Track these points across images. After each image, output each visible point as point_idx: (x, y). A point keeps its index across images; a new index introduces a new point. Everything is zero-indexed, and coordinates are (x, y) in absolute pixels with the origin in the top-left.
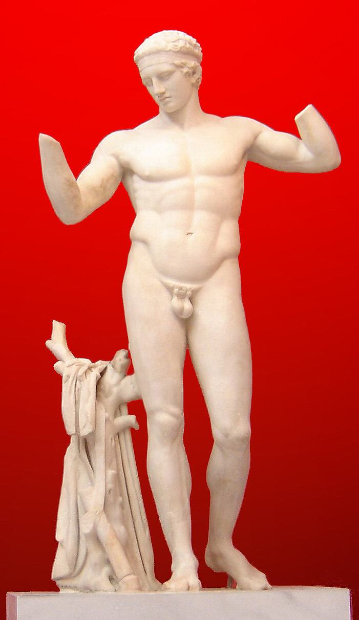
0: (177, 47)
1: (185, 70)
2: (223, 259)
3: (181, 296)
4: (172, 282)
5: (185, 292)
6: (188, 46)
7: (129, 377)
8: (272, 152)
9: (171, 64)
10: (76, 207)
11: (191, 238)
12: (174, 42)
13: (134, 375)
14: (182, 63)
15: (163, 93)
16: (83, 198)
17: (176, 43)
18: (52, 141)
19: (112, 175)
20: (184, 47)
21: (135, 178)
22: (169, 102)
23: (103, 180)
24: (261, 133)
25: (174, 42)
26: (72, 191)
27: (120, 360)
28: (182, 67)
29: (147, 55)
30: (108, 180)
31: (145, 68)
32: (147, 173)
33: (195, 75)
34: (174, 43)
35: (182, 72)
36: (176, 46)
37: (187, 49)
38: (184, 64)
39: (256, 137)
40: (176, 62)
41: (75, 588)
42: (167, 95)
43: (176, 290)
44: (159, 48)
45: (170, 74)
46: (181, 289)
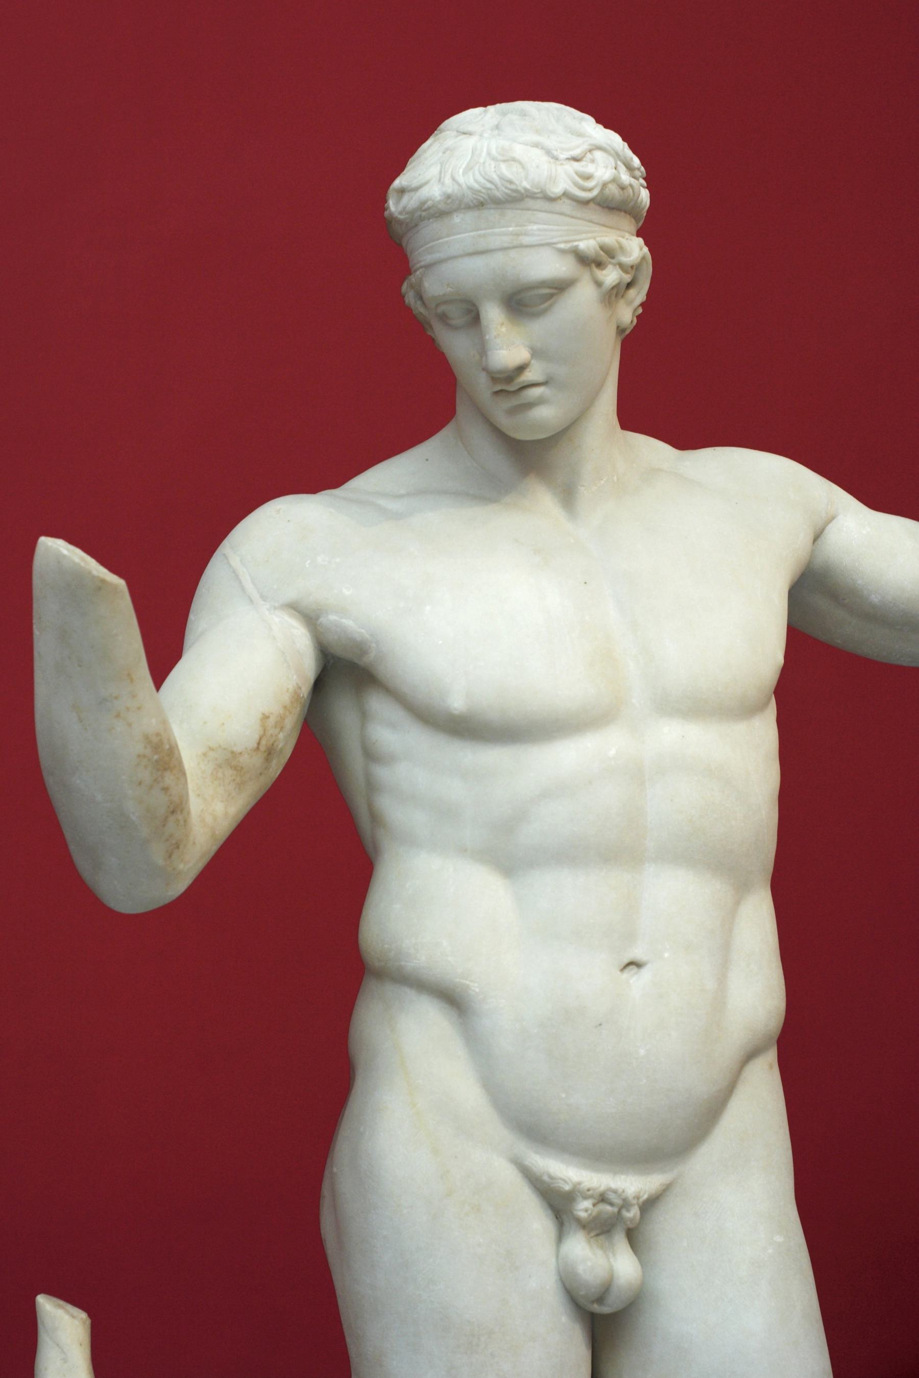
0: (590, 184)
1: (611, 276)
2: (750, 1056)
5: (616, 1210)
6: (625, 178)
8: (875, 599)
9: (562, 252)
10: (175, 847)
11: (638, 981)
12: (576, 159)
14: (603, 248)
15: (521, 369)
16: (195, 805)
17: (586, 167)
18: (103, 581)
19: (296, 695)
20: (614, 180)
21: (378, 704)
22: (540, 401)
23: (265, 717)
24: (831, 519)
25: (576, 159)
26: (166, 789)
28: (600, 265)
29: (469, 207)
30: (280, 725)
32: (457, 703)
33: (632, 292)
34: (575, 164)
35: (598, 284)
36: (588, 177)
37: (623, 188)
38: (609, 252)
39: (817, 537)
40: (583, 245)
42: (529, 376)
43: (583, 1208)
44: (526, 184)
45: (560, 287)
46: (602, 1198)
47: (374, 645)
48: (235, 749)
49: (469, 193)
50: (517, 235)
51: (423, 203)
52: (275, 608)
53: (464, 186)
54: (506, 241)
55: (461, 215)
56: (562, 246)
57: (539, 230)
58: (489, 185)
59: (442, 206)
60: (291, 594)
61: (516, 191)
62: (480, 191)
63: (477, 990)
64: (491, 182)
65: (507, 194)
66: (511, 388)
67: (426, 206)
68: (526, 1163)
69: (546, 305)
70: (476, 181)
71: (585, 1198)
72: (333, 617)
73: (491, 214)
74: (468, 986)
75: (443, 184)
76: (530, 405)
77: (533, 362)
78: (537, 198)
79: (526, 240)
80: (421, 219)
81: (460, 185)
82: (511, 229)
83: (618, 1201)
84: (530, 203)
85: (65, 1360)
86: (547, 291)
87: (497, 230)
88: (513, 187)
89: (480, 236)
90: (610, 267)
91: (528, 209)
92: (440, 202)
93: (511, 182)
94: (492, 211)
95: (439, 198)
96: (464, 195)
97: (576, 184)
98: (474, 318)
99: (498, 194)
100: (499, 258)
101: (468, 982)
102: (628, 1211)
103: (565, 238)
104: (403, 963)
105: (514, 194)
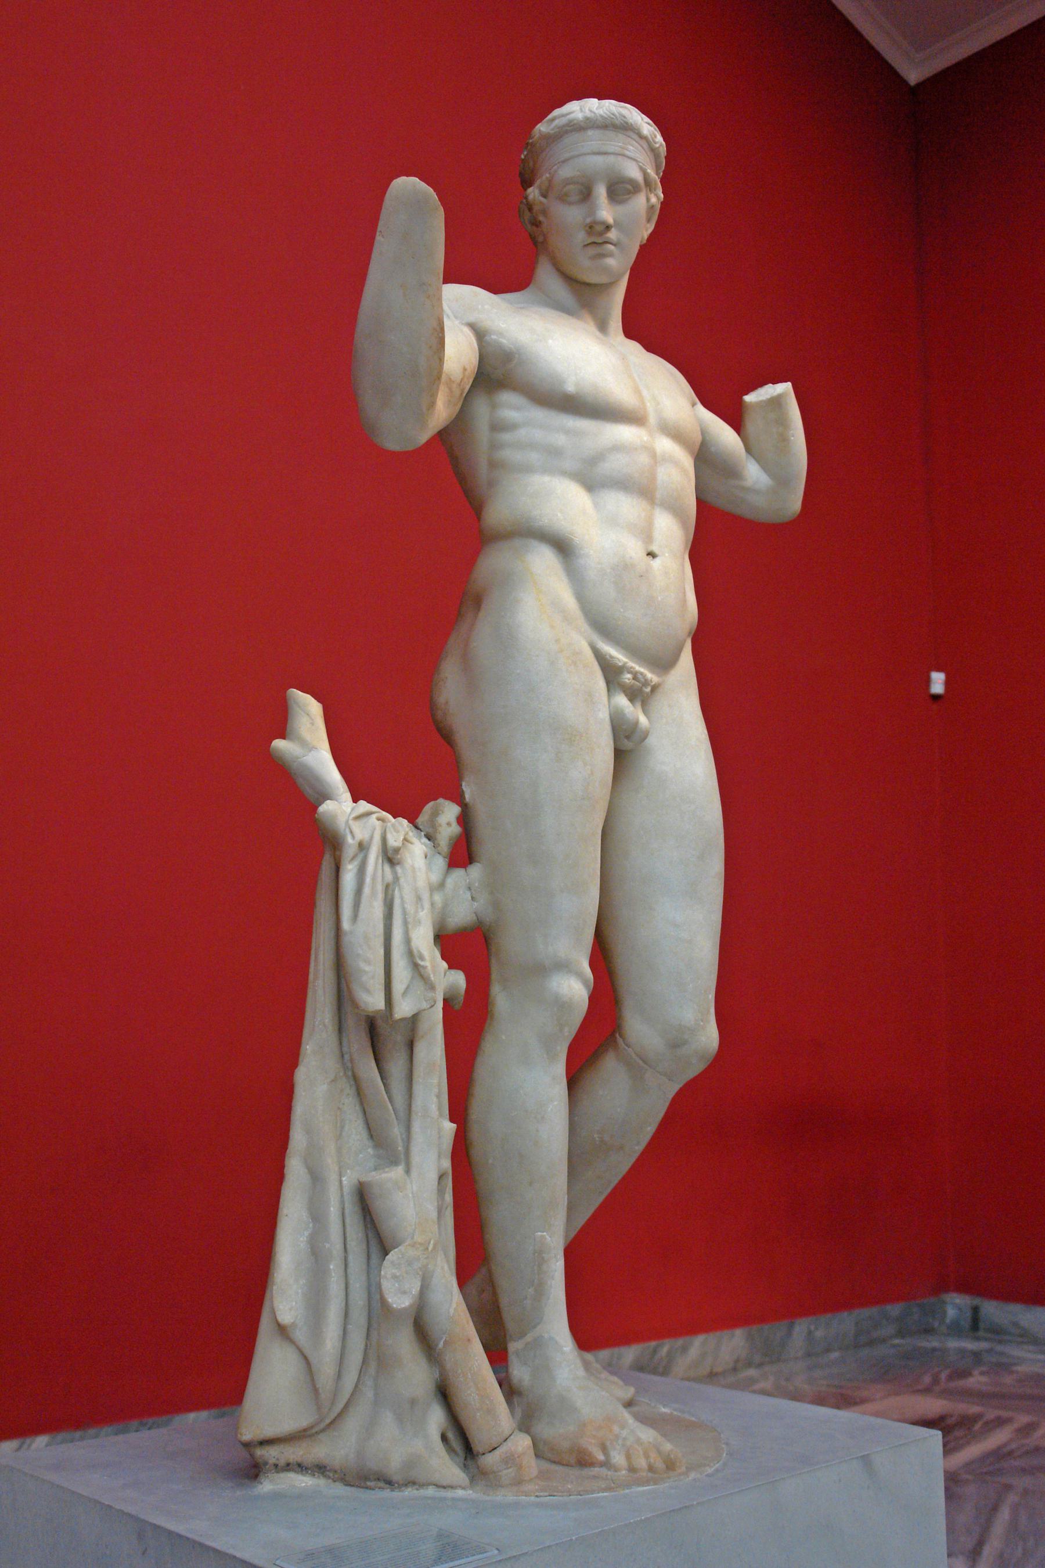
0: (657, 140)
3: (633, 695)
4: (617, 655)
7: (458, 873)
11: (656, 563)
13: (475, 871)
15: (608, 228)
22: (611, 255)
27: (449, 824)
29: (598, 127)
31: (578, 156)
35: (648, 200)
40: (649, 171)
41: (320, 1469)
43: (627, 678)
47: (517, 356)
48: (452, 378)
49: (599, 118)
50: (623, 148)
51: (570, 121)
52: (462, 324)
53: (598, 115)
54: (617, 150)
55: (593, 131)
56: (641, 164)
57: (633, 150)
58: (612, 116)
59: (582, 124)
60: (472, 319)
61: (627, 123)
62: (606, 118)
63: (578, 542)
64: (613, 114)
65: (621, 123)
66: (599, 241)
67: (572, 123)
68: (598, 646)
69: (627, 196)
70: (605, 113)
71: (629, 673)
72: (494, 337)
73: (610, 134)
74: (573, 539)
75: (585, 112)
76: (603, 256)
77: (613, 229)
78: (634, 132)
79: (627, 153)
80: (566, 132)
81: (594, 113)
82: (620, 144)
83: (643, 680)
84: (631, 133)
85: (313, 724)
86: (629, 187)
87: (612, 143)
88: (625, 120)
89: (602, 144)
90: (652, 195)
91: (629, 137)
92: (582, 121)
93: (625, 117)
94: (611, 132)
95: (581, 119)
96: (597, 120)
97: (651, 135)
98: (586, 194)
99: (617, 122)
100: (611, 159)
101: (573, 537)
102: (646, 688)
103: (643, 162)
104: (532, 524)
105: (625, 125)
